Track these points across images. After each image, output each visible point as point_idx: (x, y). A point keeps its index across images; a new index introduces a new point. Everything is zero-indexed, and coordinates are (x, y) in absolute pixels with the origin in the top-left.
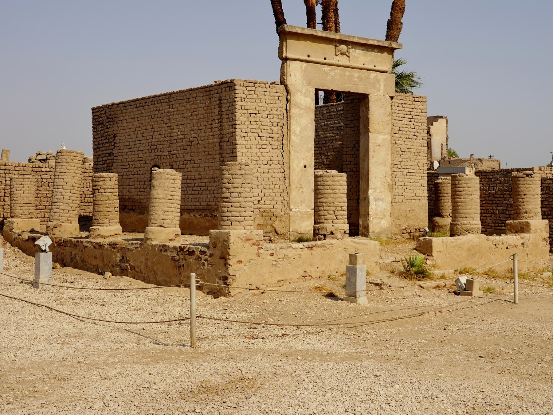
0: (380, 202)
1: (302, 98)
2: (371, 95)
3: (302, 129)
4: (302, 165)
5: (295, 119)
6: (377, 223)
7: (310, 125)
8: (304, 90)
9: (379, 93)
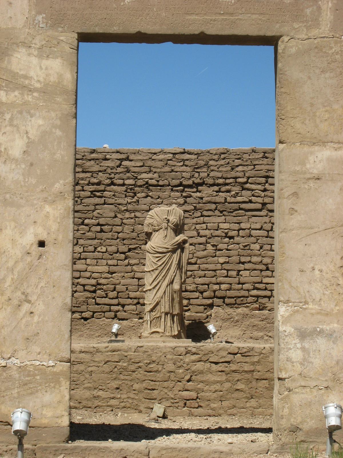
0: (321, 343)
1: (35, 61)
2: (285, 39)
3: (30, 143)
4: (30, 238)
5: (8, 116)
6: (309, 404)
7: (59, 133)
8: (38, 42)
9: (315, 32)
